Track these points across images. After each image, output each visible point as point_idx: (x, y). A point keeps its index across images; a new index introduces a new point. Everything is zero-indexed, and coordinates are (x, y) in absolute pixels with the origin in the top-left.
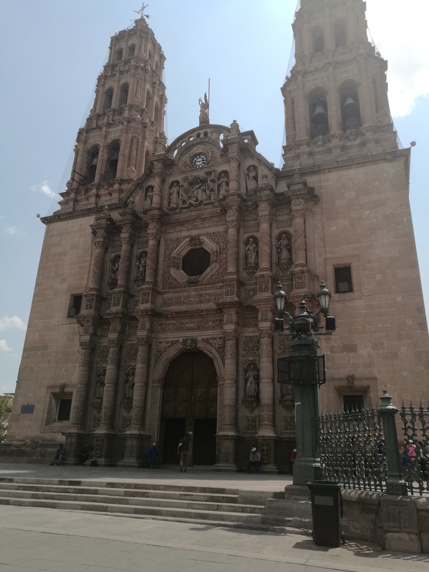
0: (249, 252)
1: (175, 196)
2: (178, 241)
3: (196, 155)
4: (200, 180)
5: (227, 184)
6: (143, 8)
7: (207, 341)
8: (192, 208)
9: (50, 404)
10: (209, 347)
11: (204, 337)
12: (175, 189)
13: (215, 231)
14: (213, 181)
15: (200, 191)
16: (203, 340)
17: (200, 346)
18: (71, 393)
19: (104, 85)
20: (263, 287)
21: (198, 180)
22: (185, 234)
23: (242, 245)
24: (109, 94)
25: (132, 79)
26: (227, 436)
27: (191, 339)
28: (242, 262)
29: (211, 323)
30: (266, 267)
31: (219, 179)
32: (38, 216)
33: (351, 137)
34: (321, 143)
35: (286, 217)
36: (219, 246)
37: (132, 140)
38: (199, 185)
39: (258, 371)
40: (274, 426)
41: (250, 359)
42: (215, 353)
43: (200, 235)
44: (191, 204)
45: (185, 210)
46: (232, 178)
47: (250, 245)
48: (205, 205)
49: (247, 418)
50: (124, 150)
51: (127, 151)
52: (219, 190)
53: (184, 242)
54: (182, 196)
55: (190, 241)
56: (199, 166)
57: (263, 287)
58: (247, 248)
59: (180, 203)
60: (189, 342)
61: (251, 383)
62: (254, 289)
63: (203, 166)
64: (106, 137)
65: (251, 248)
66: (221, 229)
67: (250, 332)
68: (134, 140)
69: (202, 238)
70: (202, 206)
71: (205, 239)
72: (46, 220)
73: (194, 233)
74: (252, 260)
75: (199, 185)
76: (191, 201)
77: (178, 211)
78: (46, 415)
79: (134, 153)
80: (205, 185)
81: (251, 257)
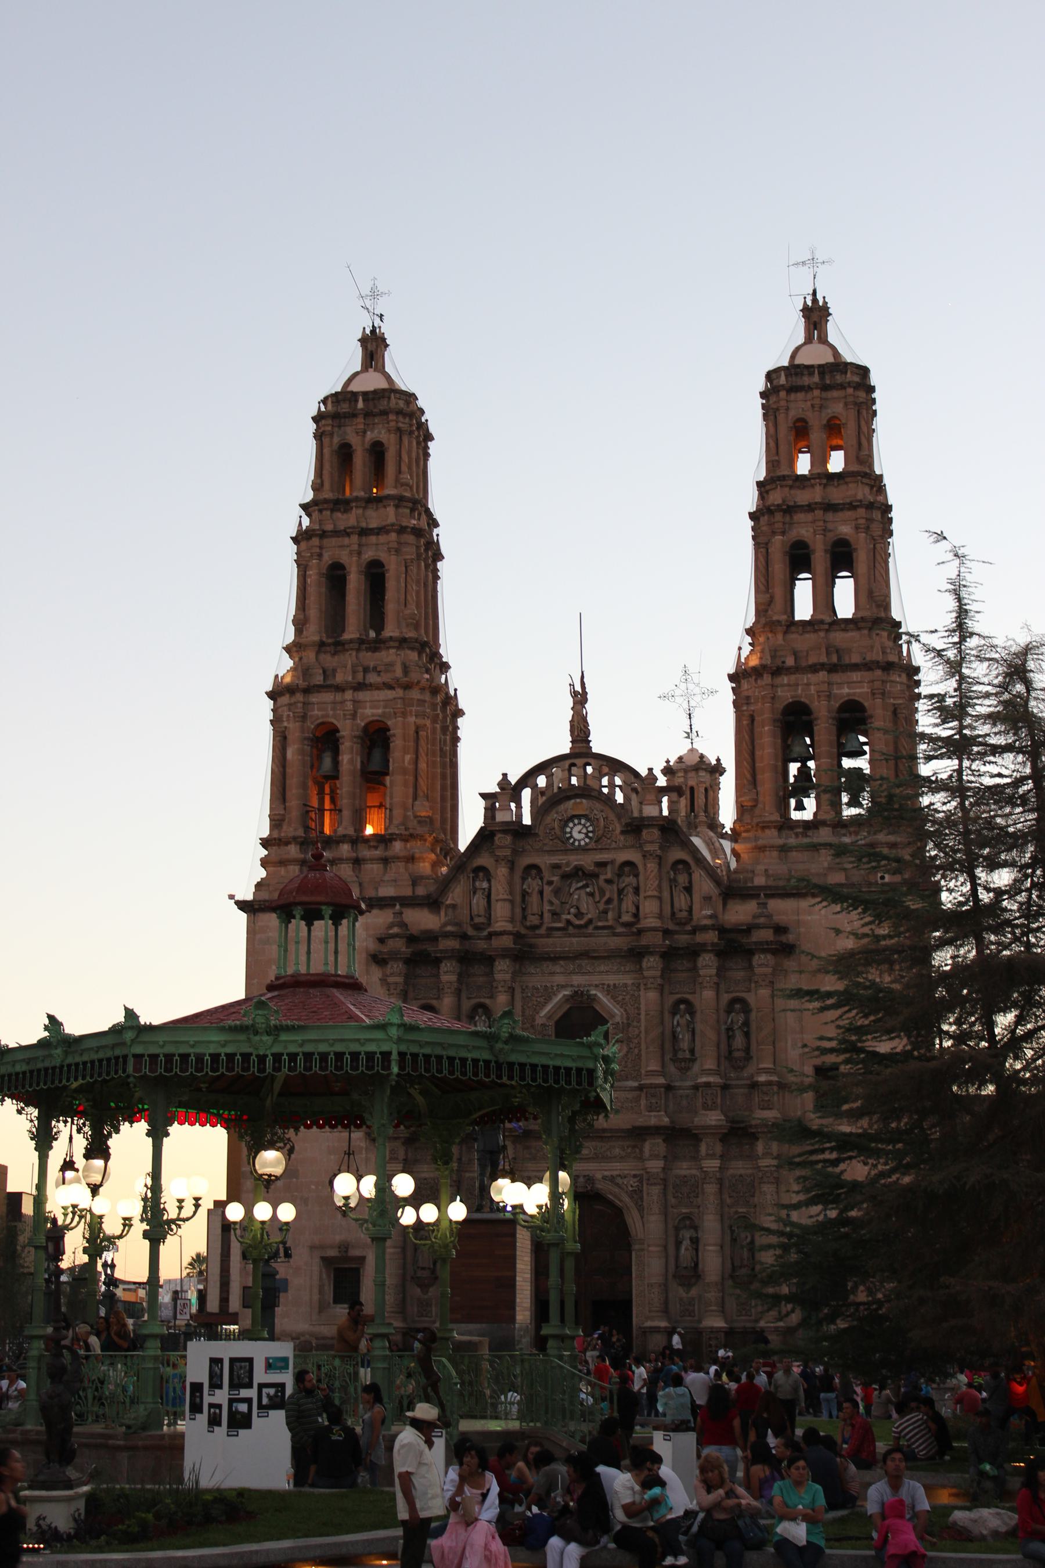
0: (679, 1029)
1: (534, 899)
2: (548, 993)
3: (571, 819)
4: (583, 872)
5: (637, 890)
6: (375, 294)
7: (612, 1179)
8: (571, 928)
9: (321, 1279)
10: (616, 1190)
11: (606, 1173)
12: (533, 884)
13: (617, 982)
14: (609, 881)
15: (582, 892)
16: (604, 1178)
17: (600, 1187)
18: (362, 1259)
19: (320, 556)
20: (710, 1103)
21: (580, 873)
22: (559, 979)
23: (667, 1015)
24: (336, 576)
25: (393, 557)
26: (659, 1327)
27: (585, 1176)
28: (668, 1045)
29: (617, 1151)
30: (712, 1067)
31: (619, 876)
32: (231, 897)
33: (852, 829)
34: (800, 830)
35: (742, 974)
36: (625, 1010)
37: (417, 733)
38: (580, 884)
39: (696, 1228)
40: (723, 1312)
41: (684, 1211)
42: (627, 1199)
43: (590, 985)
44: (568, 922)
45: (559, 933)
46: (650, 893)
47: (682, 1017)
48: (597, 928)
49: (681, 1299)
50: (400, 755)
51: (408, 758)
52: (620, 900)
53: (560, 996)
54: (551, 903)
55: (572, 996)
56: (579, 841)
57: (710, 1103)
58: (675, 1023)
59: (547, 916)
60: (581, 1179)
61: (686, 1249)
62: (687, 1096)
63: (586, 844)
64: (354, 716)
65: (683, 1022)
66: (628, 980)
67: (684, 1169)
68: (421, 733)
69: (593, 992)
70: (590, 929)
71: (600, 995)
72: (243, 905)
73: (578, 980)
74: (685, 1045)
75: (580, 884)
76: (568, 917)
77: (542, 931)
78: (316, 1297)
79: (422, 765)
80: (593, 884)
81: (683, 1039)
